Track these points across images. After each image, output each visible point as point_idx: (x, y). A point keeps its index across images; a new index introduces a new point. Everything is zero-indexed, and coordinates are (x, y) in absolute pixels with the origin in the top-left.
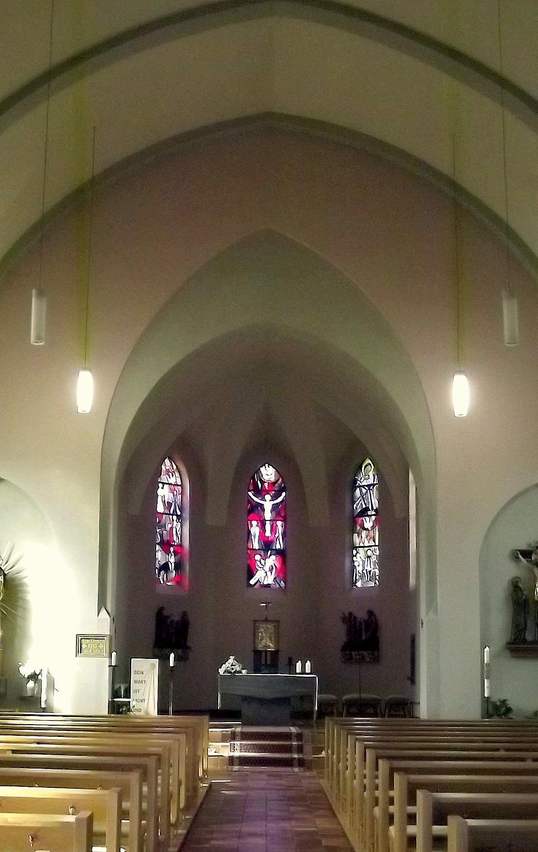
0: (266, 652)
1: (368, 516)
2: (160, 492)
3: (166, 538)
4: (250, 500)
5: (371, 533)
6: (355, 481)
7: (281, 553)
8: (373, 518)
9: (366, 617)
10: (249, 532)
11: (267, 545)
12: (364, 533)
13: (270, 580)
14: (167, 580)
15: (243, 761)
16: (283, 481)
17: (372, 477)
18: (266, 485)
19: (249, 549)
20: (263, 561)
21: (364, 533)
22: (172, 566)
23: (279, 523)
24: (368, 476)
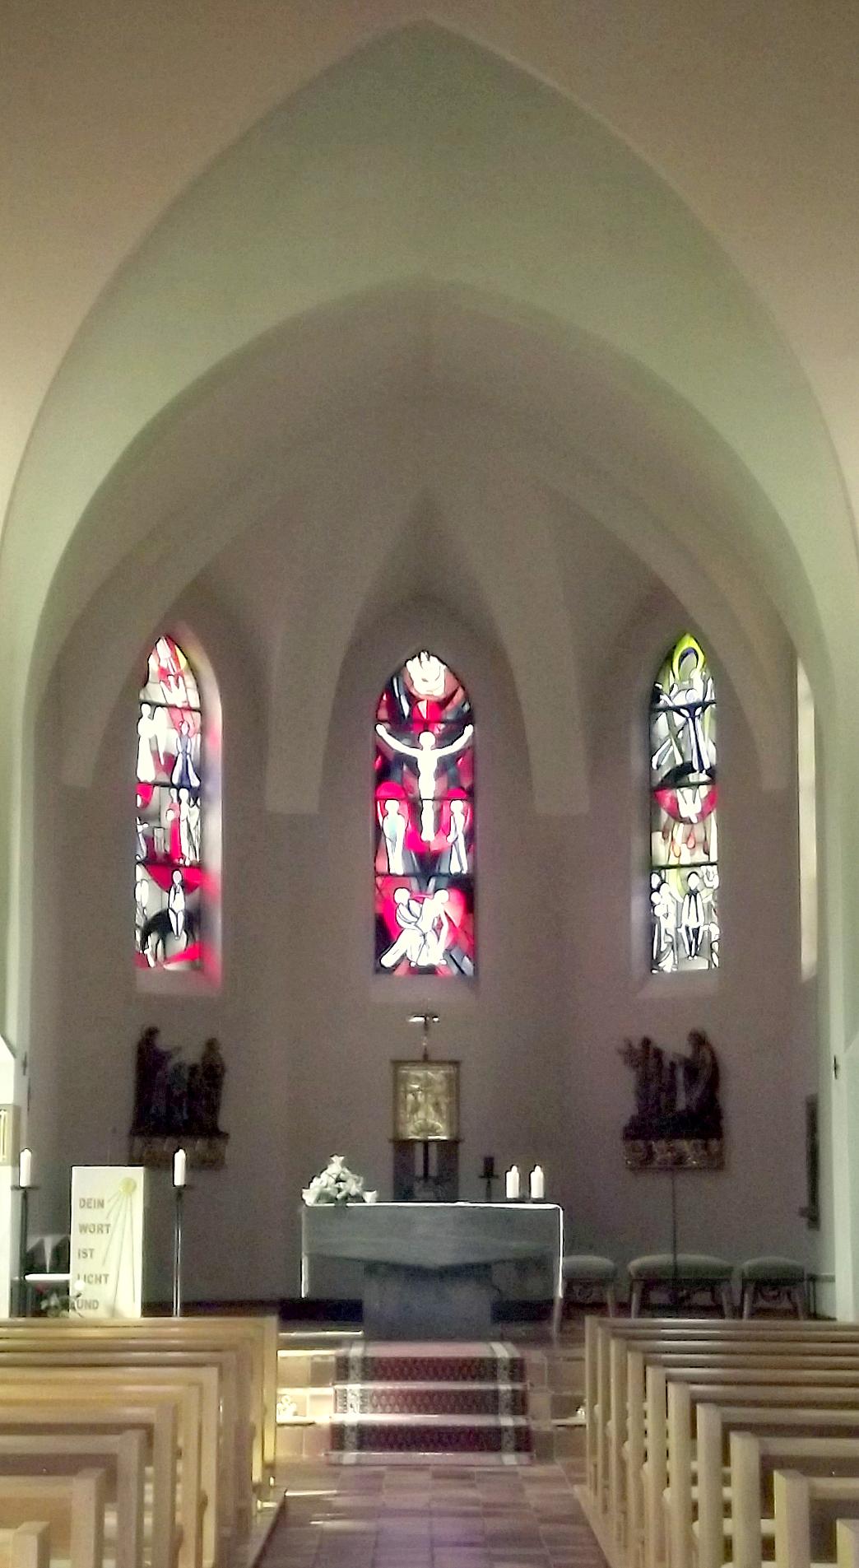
0: (426, 1143)
1: (689, 785)
2: (146, 728)
3: (162, 846)
4: (380, 750)
5: (699, 832)
6: (656, 695)
7: (464, 887)
8: (704, 791)
9: (686, 1050)
10: (379, 830)
11: (427, 863)
12: (679, 831)
14: (163, 959)
15: (370, 1438)
16: (467, 698)
17: (698, 684)
18: (422, 707)
19: (377, 874)
20: (414, 905)
21: (679, 831)
22: (178, 922)
23: (458, 806)
24: (688, 682)
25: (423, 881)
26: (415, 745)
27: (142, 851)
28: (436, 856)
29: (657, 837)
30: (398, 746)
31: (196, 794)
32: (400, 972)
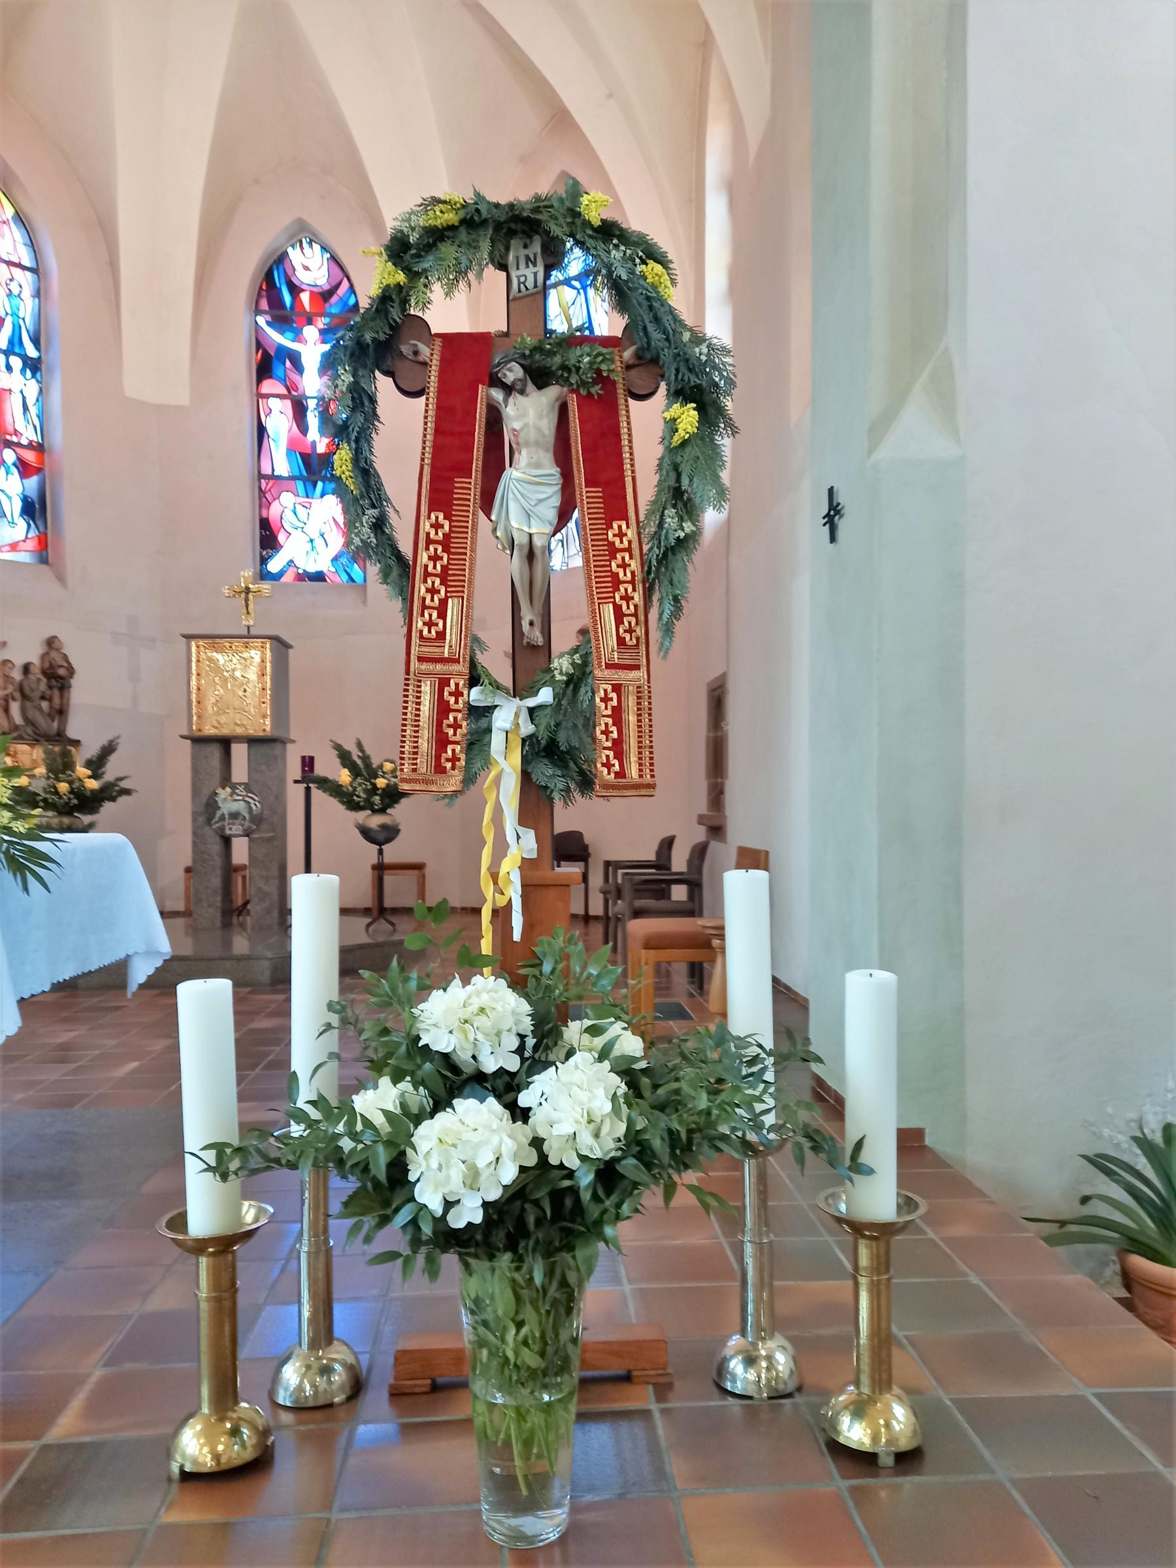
10: (261, 431)
13: (321, 562)
18: (305, 297)
19: (261, 476)
25: (310, 487)
26: (299, 338)
31: (33, 366)
32: (288, 578)
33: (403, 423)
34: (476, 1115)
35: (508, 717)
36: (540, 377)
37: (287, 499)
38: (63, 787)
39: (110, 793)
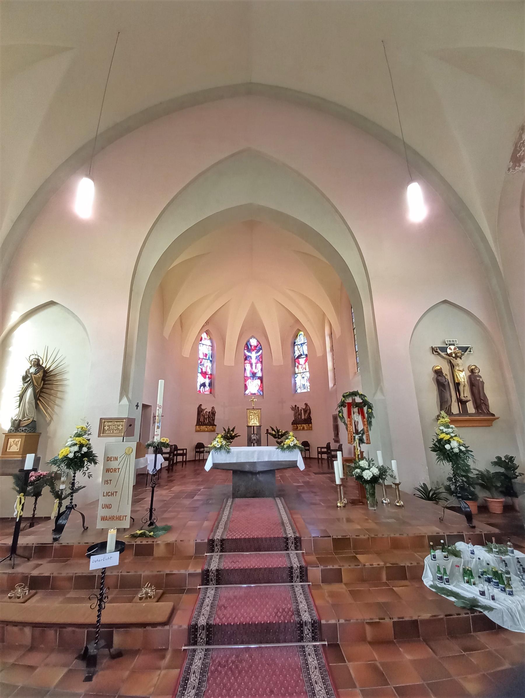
0: (254, 426)
3: (204, 370)
6: (295, 343)
7: (261, 379)
8: (305, 359)
10: (245, 369)
18: (253, 347)
21: (300, 366)
22: (207, 384)
23: (259, 365)
27: (200, 371)
28: (256, 373)
29: (296, 368)
30: (248, 354)
31: (211, 361)
33: (345, 410)
34: (366, 471)
35: (357, 437)
36: (356, 407)
37: (249, 380)
38: (229, 435)
39: (236, 436)
